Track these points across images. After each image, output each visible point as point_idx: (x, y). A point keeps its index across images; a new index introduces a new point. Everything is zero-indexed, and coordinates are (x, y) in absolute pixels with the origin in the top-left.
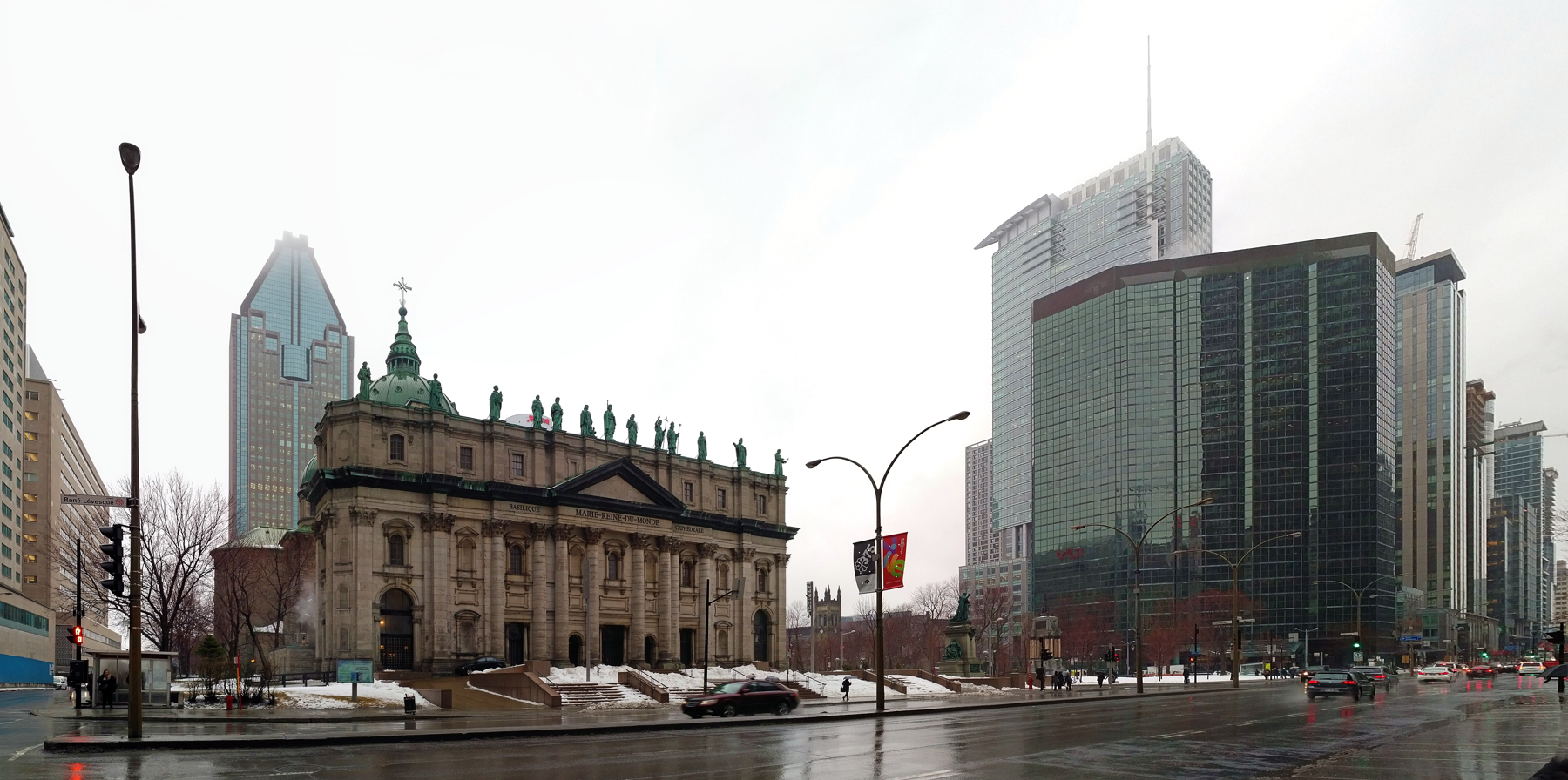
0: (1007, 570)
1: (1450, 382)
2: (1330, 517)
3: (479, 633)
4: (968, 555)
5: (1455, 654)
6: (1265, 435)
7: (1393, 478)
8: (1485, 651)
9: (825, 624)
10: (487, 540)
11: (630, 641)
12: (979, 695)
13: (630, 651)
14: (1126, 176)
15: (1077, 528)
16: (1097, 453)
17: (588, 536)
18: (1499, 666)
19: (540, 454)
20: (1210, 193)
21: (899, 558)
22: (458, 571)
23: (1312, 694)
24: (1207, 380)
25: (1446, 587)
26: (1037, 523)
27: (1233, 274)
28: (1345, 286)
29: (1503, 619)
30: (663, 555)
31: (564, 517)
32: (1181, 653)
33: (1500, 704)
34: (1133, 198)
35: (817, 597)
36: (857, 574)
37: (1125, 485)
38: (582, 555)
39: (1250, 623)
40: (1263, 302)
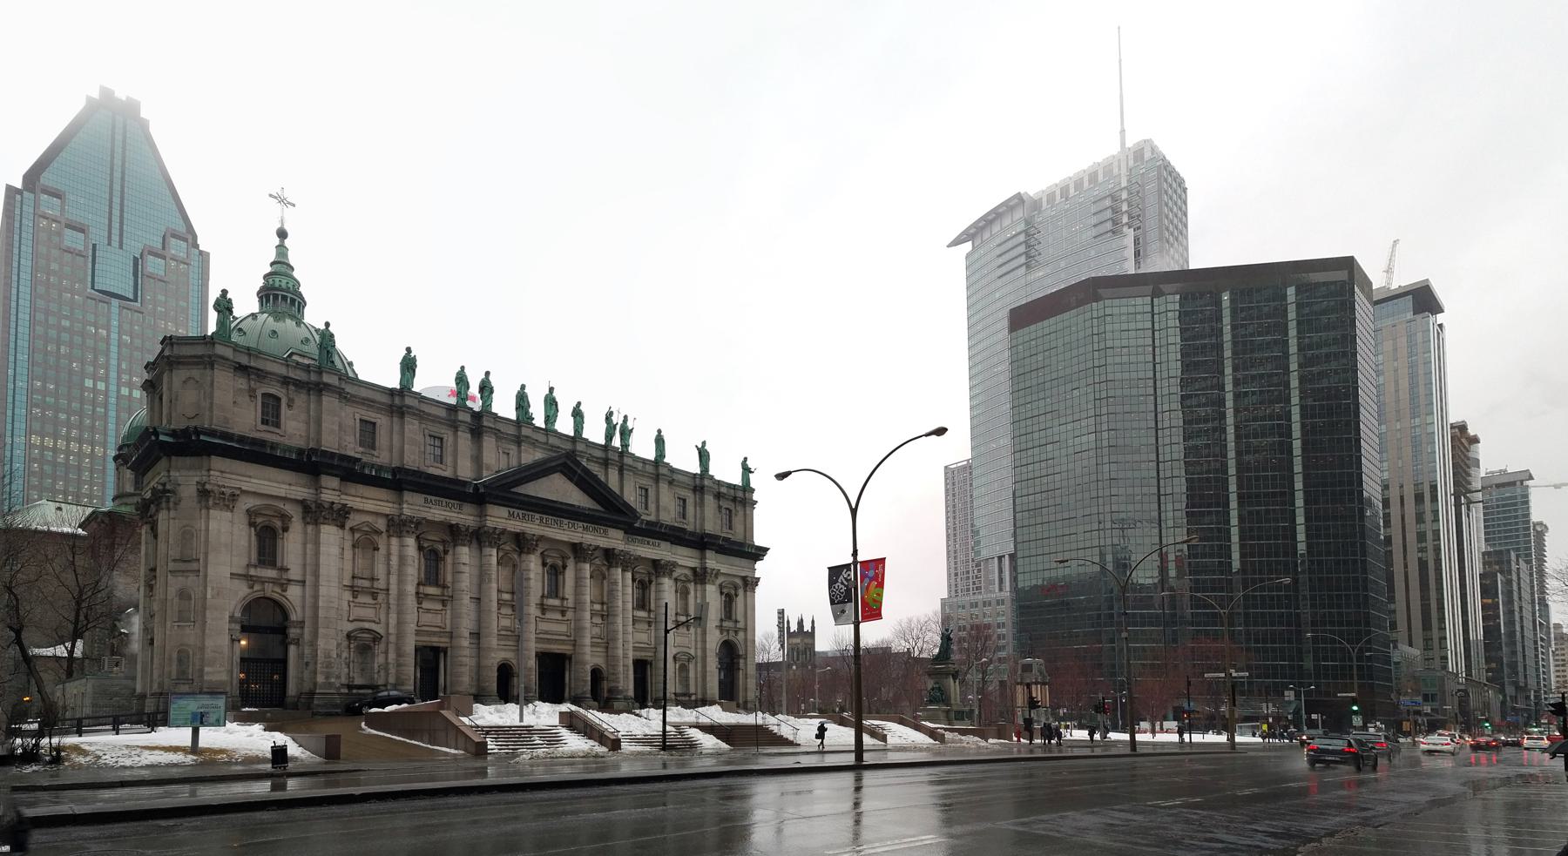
0: (990, 604)
1: (1433, 423)
2: (1320, 563)
3: (380, 659)
4: (950, 586)
5: (1457, 722)
6: (1249, 470)
7: (1382, 524)
8: (1487, 721)
9: (798, 660)
10: (394, 541)
11: (573, 672)
12: (964, 747)
13: (573, 686)
14: (1100, 179)
15: (1061, 562)
16: (1079, 481)
17: (522, 543)
18: (1503, 738)
19: (465, 439)
20: (1185, 203)
21: (877, 586)
22: (353, 577)
23: (1313, 761)
24: (1189, 407)
25: (1443, 647)
26: (1020, 554)
27: (1211, 293)
28: (1324, 312)
29: (1503, 685)
30: (613, 570)
31: (492, 519)
32: (1174, 708)
33: (1507, 782)
34: (1108, 203)
35: (789, 628)
36: (832, 602)
37: (1108, 517)
38: (514, 566)
39: (1243, 677)
40: (1242, 325)
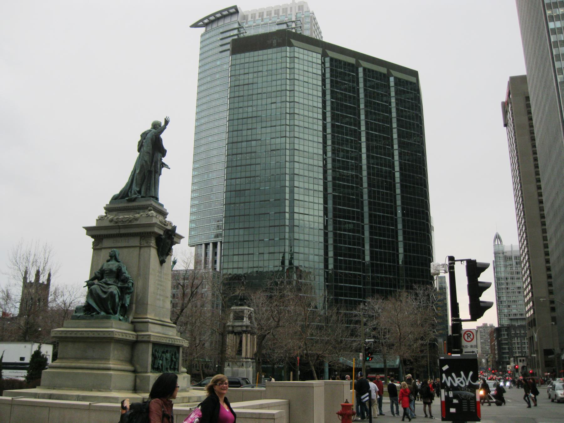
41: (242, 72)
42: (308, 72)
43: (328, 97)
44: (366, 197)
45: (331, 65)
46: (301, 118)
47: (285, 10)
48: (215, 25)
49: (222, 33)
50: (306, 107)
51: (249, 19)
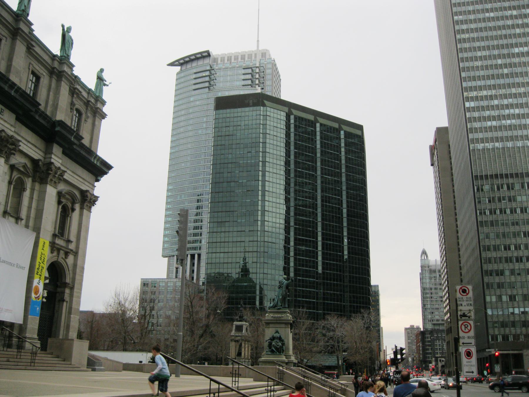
34: (250, 71)
41: (224, 125)
42: (277, 127)
43: (292, 148)
44: (320, 229)
45: (295, 121)
46: (271, 165)
47: (250, 56)
48: (189, 66)
49: (195, 73)
50: (275, 156)
51: (219, 62)
